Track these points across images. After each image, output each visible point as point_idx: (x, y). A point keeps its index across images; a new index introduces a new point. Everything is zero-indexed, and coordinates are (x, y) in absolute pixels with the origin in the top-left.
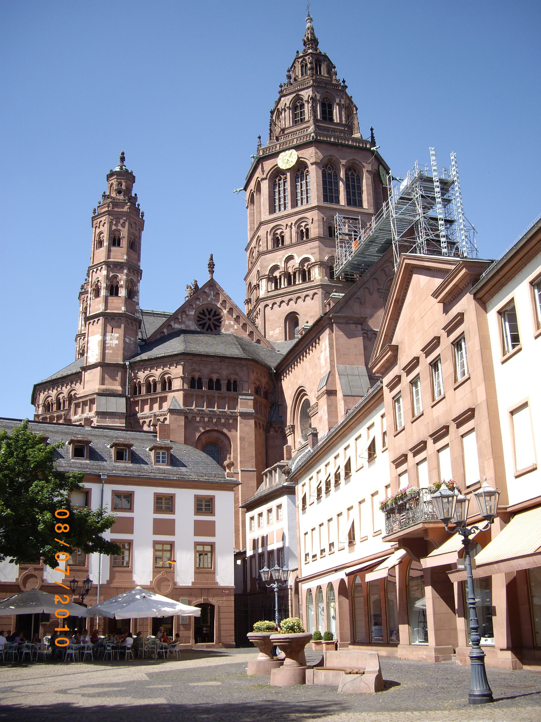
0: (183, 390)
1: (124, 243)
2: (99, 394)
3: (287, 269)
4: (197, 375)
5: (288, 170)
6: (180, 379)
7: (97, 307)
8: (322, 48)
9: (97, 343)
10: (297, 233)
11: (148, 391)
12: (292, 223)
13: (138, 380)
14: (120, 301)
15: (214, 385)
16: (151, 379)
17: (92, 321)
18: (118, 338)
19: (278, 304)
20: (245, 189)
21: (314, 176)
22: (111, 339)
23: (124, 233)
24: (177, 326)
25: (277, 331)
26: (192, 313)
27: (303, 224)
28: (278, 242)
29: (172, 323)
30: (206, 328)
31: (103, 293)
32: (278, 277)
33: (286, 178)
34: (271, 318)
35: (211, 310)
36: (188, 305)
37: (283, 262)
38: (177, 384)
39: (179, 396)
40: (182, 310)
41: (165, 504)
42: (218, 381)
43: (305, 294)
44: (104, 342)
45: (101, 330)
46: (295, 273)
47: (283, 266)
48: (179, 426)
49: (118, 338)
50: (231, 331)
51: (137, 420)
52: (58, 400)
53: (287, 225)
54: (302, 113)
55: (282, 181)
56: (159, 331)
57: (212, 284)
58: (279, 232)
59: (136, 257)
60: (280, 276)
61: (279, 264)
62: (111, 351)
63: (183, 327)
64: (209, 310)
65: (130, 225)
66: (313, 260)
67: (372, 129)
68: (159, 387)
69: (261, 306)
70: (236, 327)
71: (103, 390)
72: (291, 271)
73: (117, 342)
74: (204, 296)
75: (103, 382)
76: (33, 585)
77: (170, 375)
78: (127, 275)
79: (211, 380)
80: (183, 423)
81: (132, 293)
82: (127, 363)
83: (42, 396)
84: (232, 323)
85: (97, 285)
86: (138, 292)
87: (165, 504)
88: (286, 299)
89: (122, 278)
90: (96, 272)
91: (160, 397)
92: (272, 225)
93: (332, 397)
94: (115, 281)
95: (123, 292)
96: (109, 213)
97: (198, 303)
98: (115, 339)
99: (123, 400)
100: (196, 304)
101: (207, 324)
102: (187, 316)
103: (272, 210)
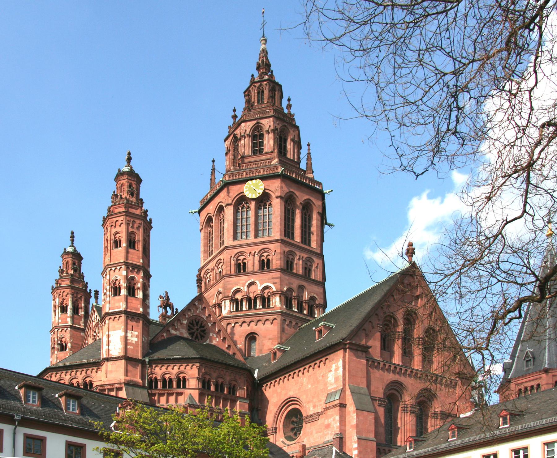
0: (199, 389)
3: (249, 293)
6: (195, 379)
7: (117, 305)
9: (119, 338)
10: (259, 261)
11: (164, 386)
12: (255, 252)
13: (154, 376)
14: (138, 302)
16: (167, 376)
17: (113, 317)
18: (137, 336)
19: (240, 324)
22: (132, 337)
27: (265, 254)
30: (194, 337)
32: (240, 299)
35: (199, 321)
37: (246, 287)
38: (193, 383)
39: (195, 394)
44: (126, 338)
45: (123, 327)
47: (246, 290)
50: (214, 343)
53: (250, 253)
55: (245, 210)
58: (241, 258)
59: (147, 262)
60: (242, 299)
61: (242, 288)
62: (132, 347)
64: (197, 321)
68: (175, 384)
71: (128, 381)
72: (252, 296)
73: (136, 339)
74: (194, 309)
75: (126, 373)
77: (184, 375)
82: (147, 360)
84: (215, 336)
85: (115, 283)
86: (149, 296)
88: (248, 320)
90: (114, 271)
91: (176, 393)
93: (343, 408)
94: (132, 282)
98: (135, 337)
100: (188, 315)
101: (195, 334)
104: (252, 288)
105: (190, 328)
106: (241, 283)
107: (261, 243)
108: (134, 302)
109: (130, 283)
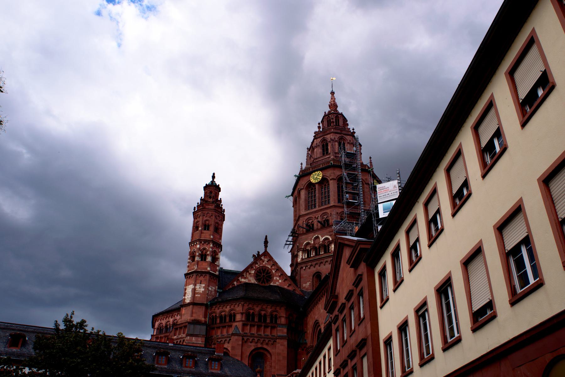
1: (212, 228)
2: (189, 323)
4: (251, 311)
5: (316, 183)
8: (340, 110)
15: (262, 318)
16: (223, 313)
18: (204, 287)
20: (292, 195)
21: (333, 186)
24: (243, 280)
25: (308, 284)
26: (253, 272)
27: (325, 217)
28: (310, 229)
29: (240, 278)
31: (197, 259)
33: (315, 188)
34: (304, 276)
36: (250, 266)
39: (239, 325)
40: (246, 270)
42: (265, 315)
43: (325, 260)
46: (319, 247)
48: (238, 344)
49: (204, 287)
50: (277, 284)
54: (327, 149)
57: (266, 254)
58: (310, 221)
63: (246, 281)
66: (331, 239)
67: (370, 158)
68: (228, 319)
69: (298, 268)
70: (280, 281)
72: (317, 246)
73: (203, 290)
79: (260, 315)
80: (240, 343)
82: (209, 303)
83: (157, 324)
84: (278, 279)
88: (314, 263)
92: (306, 217)
94: (204, 251)
95: (209, 259)
97: (257, 266)
99: (205, 327)
102: (250, 274)
103: (307, 208)
104: (317, 241)
105: (257, 276)
106: (310, 239)
107: (321, 210)
108: (204, 264)
109: (202, 252)
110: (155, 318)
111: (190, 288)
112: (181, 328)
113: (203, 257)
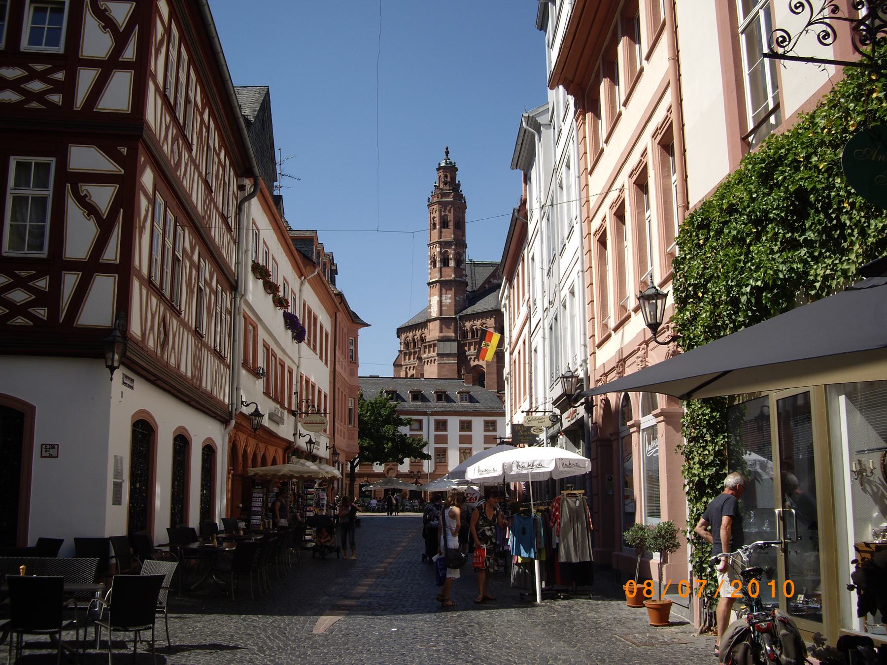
1: (451, 224)
2: (439, 341)
11: (473, 336)
23: (451, 217)
31: (438, 265)
41: (466, 426)
51: (466, 357)
52: (414, 340)
56: (483, 286)
65: (455, 210)
75: (441, 332)
76: (392, 474)
78: (455, 250)
81: (459, 261)
83: (403, 336)
87: (466, 426)
89: (451, 253)
95: (452, 264)
96: (439, 203)
98: (448, 299)
99: (456, 344)
110: (400, 331)
111: (435, 300)
112: (430, 346)
113: (445, 262)
